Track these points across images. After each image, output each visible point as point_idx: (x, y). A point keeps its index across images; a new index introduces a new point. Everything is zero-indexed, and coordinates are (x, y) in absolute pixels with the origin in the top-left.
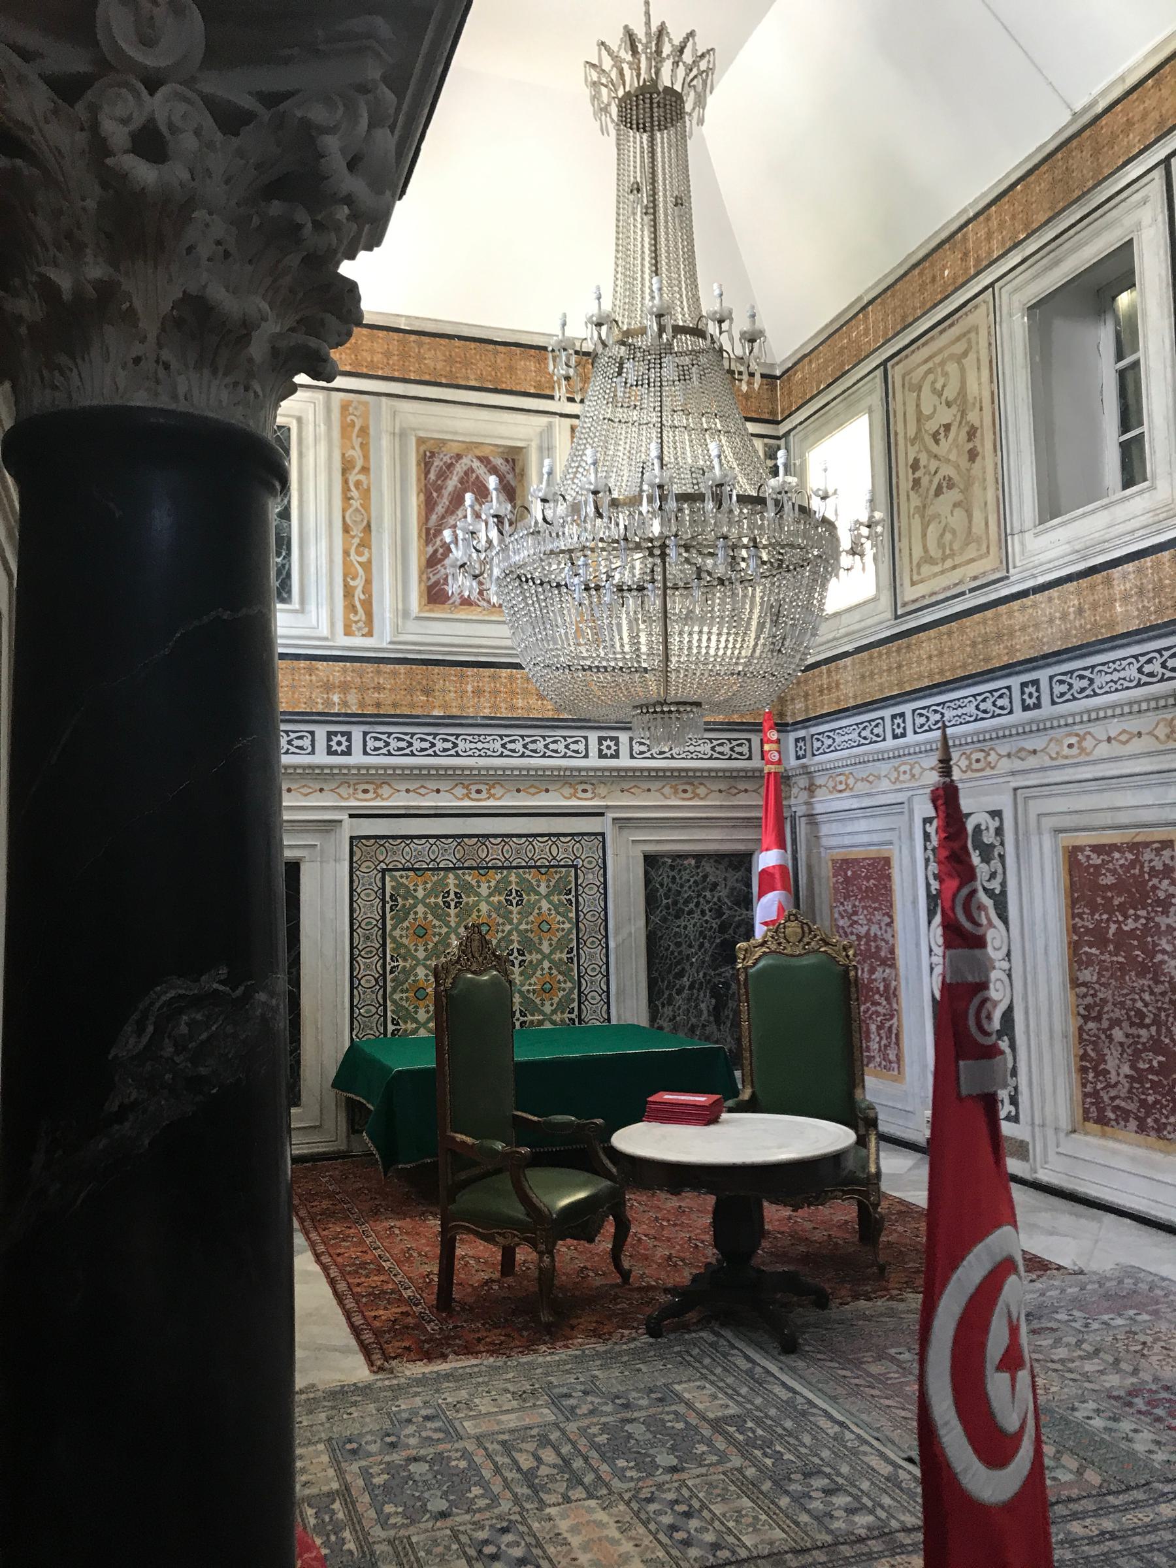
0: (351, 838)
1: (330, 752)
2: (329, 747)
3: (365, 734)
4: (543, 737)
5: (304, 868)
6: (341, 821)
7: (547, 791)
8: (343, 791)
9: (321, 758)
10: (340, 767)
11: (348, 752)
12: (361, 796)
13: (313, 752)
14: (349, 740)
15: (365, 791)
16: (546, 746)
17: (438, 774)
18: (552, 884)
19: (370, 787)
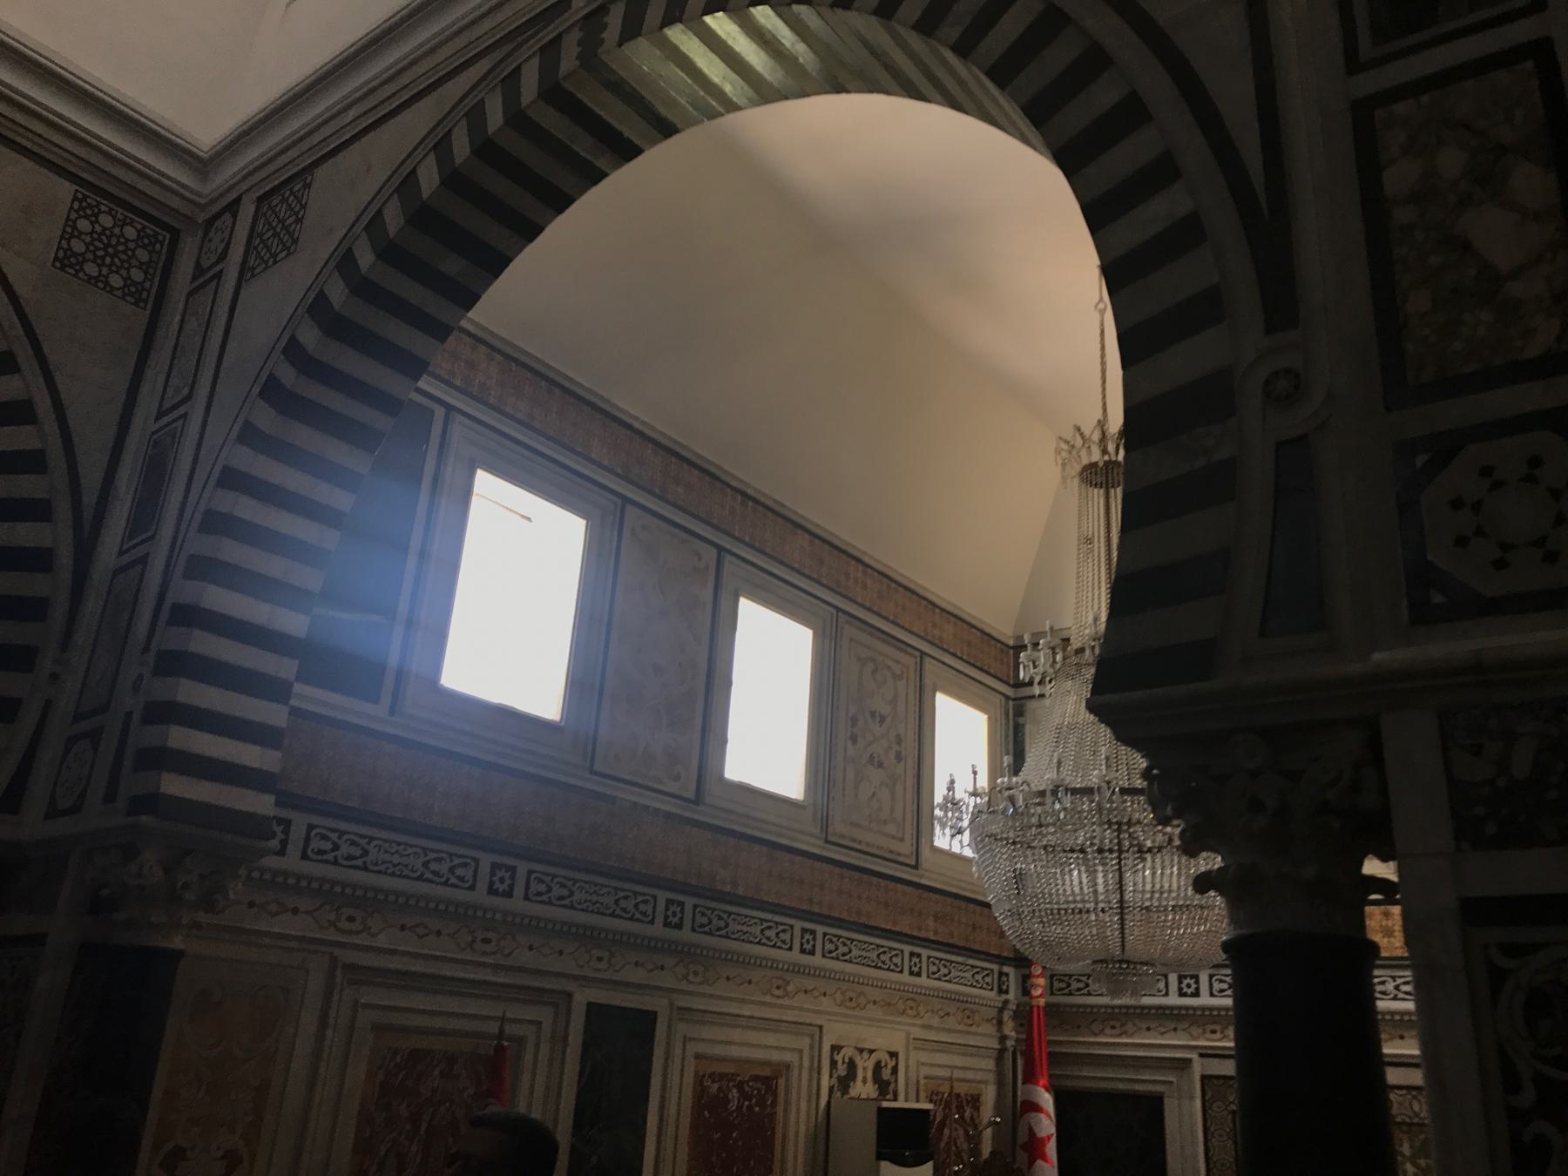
0: (1203, 1077)
1: (1182, 994)
2: (1180, 989)
3: (1211, 976)
4: (1394, 978)
5: (1166, 1101)
6: (1190, 1061)
7: (1402, 1037)
8: (1196, 1031)
9: (1173, 1000)
10: (1187, 1008)
11: (1196, 994)
12: (1208, 1035)
13: (1167, 994)
14: (1197, 982)
15: (1213, 1032)
16: (1397, 988)
17: (1392, 1020)
18: (1417, 1144)
19: (1217, 1027)
